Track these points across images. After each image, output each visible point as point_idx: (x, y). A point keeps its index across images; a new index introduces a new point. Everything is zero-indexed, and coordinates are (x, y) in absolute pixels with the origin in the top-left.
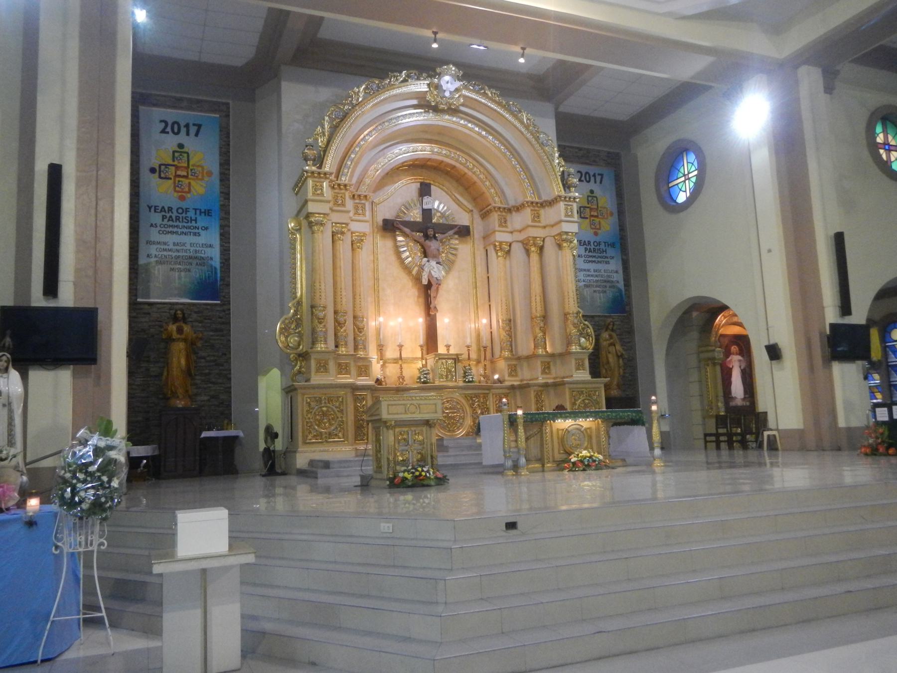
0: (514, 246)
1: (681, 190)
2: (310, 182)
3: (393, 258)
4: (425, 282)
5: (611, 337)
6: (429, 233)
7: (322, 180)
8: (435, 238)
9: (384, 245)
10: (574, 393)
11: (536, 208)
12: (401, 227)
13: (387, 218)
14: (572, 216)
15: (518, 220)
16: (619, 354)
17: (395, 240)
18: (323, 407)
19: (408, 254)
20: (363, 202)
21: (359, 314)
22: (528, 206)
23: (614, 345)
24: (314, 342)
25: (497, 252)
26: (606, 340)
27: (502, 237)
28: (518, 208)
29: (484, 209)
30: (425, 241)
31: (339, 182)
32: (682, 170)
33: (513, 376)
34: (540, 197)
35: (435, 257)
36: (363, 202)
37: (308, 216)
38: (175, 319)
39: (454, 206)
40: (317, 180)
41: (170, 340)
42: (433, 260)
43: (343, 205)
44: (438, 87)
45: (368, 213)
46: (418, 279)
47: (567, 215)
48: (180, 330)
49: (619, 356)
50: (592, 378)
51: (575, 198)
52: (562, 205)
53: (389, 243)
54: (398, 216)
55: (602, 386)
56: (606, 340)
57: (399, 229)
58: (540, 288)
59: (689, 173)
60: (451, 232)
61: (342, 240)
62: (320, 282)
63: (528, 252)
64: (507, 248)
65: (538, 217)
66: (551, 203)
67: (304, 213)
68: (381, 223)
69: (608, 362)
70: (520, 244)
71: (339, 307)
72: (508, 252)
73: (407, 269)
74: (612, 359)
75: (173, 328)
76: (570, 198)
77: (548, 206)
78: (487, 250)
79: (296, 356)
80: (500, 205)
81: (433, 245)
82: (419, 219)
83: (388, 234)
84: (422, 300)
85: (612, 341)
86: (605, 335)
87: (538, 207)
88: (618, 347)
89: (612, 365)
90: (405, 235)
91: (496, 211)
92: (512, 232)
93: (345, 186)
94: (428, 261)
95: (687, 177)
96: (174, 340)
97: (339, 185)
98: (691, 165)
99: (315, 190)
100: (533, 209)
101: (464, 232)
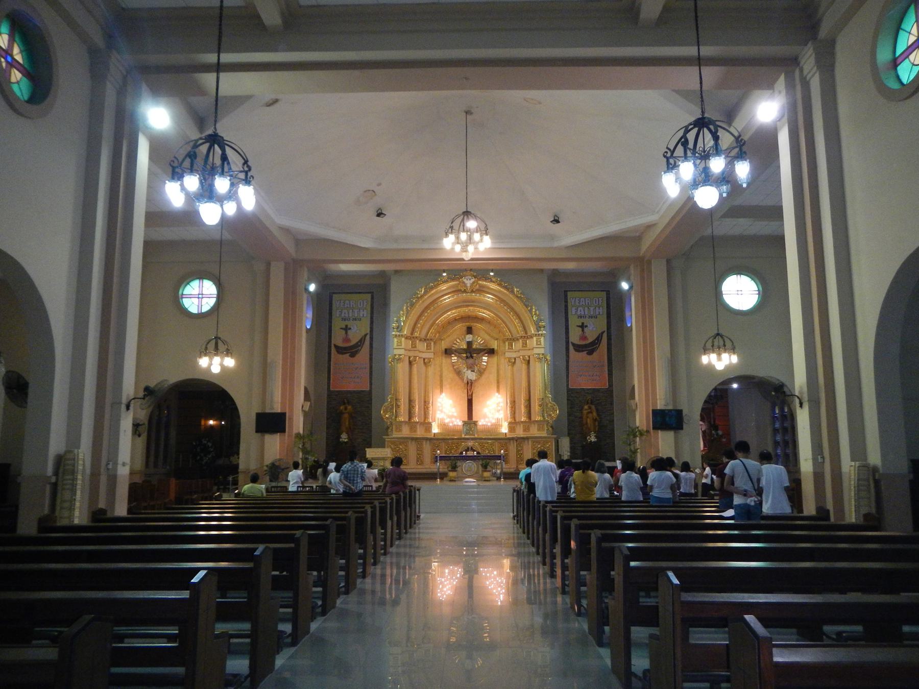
3: (452, 369)
4: (465, 381)
5: (590, 408)
8: (472, 357)
9: (445, 361)
10: (534, 444)
12: (455, 353)
15: (517, 345)
21: (427, 400)
23: (592, 413)
26: (586, 410)
27: (508, 355)
28: (518, 340)
31: (413, 336)
34: (526, 333)
35: (471, 368)
38: (344, 403)
41: (342, 413)
43: (415, 347)
44: (464, 283)
47: (537, 344)
48: (346, 409)
49: (595, 420)
51: (542, 334)
52: (535, 338)
53: (448, 360)
55: (553, 439)
56: (586, 410)
58: (527, 384)
64: (513, 360)
66: (532, 337)
68: (443, 349)
69: (587, 423)
71: (412, 398)
72: (515, 361)
75: (342, 408)
76: (539, 334)
81: (471, 361)
82: (465, 347)
84: (466, 391)
85: (589, 410)
86: (586, 407)
88: (595, 414)
89: (589, 426)
90: (456, 356)
93: (416, 337)
96: (344, 413)
97: (413, 337)
101: (491, 352)
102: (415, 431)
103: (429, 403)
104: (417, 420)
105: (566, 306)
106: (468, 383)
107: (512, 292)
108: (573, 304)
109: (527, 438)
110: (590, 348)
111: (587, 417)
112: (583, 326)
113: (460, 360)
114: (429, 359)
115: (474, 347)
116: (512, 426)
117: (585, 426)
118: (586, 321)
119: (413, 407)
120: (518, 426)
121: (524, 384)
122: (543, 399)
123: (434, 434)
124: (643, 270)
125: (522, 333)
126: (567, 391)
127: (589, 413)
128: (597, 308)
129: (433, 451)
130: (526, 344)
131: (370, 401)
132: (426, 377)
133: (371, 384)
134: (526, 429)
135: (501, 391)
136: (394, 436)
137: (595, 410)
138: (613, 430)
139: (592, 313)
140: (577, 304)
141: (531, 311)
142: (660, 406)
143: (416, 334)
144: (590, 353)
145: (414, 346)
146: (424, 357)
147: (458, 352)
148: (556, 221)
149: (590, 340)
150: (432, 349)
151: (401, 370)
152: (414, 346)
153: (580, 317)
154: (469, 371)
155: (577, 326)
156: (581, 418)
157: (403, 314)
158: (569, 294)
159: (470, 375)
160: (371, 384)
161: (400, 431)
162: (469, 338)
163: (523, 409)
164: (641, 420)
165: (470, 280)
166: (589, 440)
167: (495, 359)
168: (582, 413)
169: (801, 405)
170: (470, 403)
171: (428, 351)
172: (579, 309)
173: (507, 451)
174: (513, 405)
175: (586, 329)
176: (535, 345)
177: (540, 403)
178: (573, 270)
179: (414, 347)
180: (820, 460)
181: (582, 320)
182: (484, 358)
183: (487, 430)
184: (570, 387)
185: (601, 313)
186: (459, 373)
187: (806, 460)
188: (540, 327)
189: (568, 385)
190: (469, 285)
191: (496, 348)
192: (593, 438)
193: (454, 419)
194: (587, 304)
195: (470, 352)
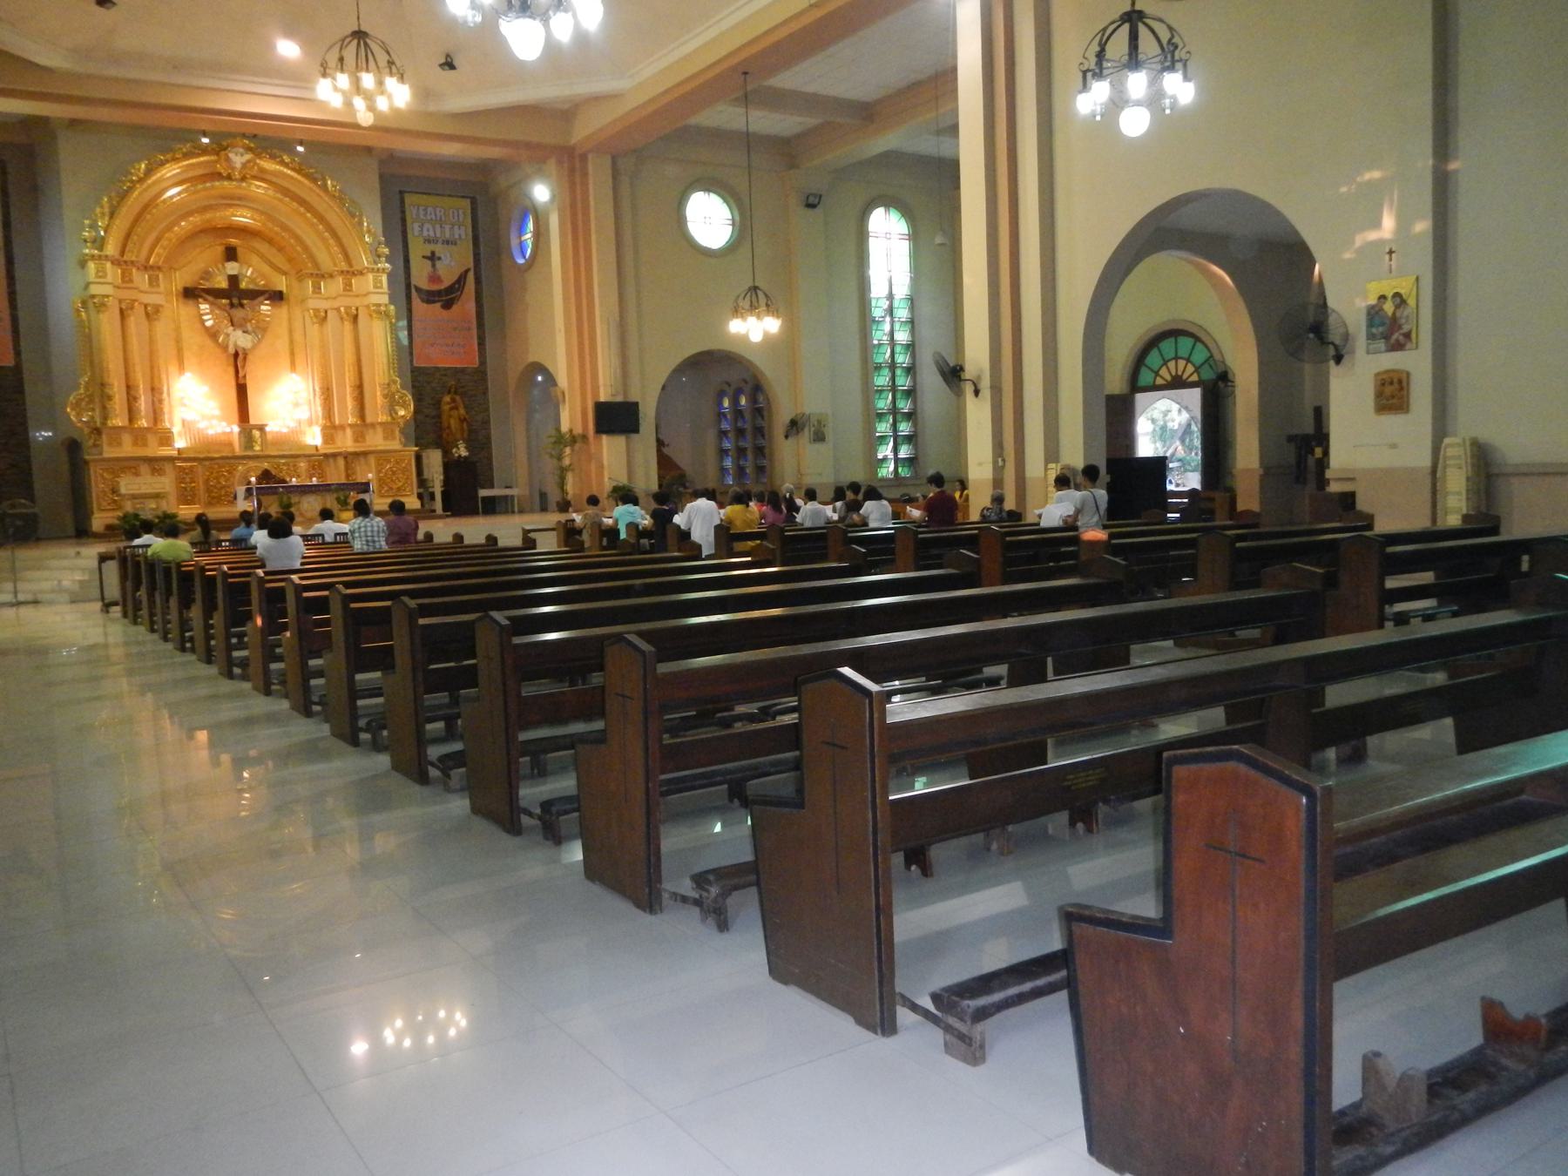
0: (329, 312)
3: (198, 325)
4: (231, 350)
5: (453, 400)
7: (104, 262)
8: (242, 306)
9: (185, 310)
10: (381, 462)
12: (204, 295)
13: (188, 285)
14: (381, 287)
16: (462, 417)
17: (199, 308)
22: (340, 275)
26: (448, 403)
27: (313, 303)
28: (331, 276)
31: (125, 258)
33: (329, 444)
34: (351, 265)
39: (266, 269)
43: (131, 281)
46: (225, 348)
47: (375, 287)
49: (462, 420)
51: (383, 269)
56: (448, 403)
57: (201, 297)
60: (261, 299)
64: (323, 314)
68: (180, 288)
69: (449, 424)
70: (335, 312)
71: (130, 384)
72: (325, 318)
74: (453, 423)
76: (378, 269)
80: (312, 272)
81: (238, 314)
82: (224, 284)
83: (191, 302)
84: (231, 370)
85: (453, 405)
86: (447, 399)
88: (462, 411)
89: (454, 430)
97: (125, 262)
101: (277, 297)
102: (145, 445)
103: (161, 393)
104: (144, 423)
105: (404, 220)
106: (236, 355)
107: (324, 187)
108: (414, 216)
109: (365, 454)
110: (446, 297)
111: (450, 416)
112: (432, 258)
113: (217, 312)
114: (157, 309)
115: (243, 285)
116: (331, 430)
117: (447, 431)
118: (439, 249)
119: (136, 399)
120: (340, 433)
121: (349, 357)
122: (388, 384)
123: (179, 450)
124: (572, 171)
125: (344, 266)
126: (412, 372)
127: (451, 409)
128: (456, 227)
129: (181, 482)
130: (351, 285)
131: (19, 389)
132: (152, 341)
133: (18, 353)
134: (359, 437)
135: (299, 367)
136: (106, 455)
137: (462, 406)
138: (488, 438)
139: (447, 235)
140: (422, 217)
141: (361, 224)
142: (602, 399)
143: (128, 257)
144: (448, 305)
145: (127, 279)
146: (146, 301)
147: (216, 294)
148: (449, 65)
149: (446, 283)
150: (162, 285)
151: (107, 326)
152: (127, 279)
153: (428, 241)
154: (239, 333)
155: (424, 257)
156: (439, 416)
157: (103, 214)
158: (408, 199)
159: (240, 339)
160: (18, 353)
161: (120, 444)
162: (232, 268)
163: (350, 404)
164: (572, 417)
165: (242, 155)
166: (456, 455)
167: (283, 311)
168: (439, 408)
169: (977, 392)
170: (242, 391)
171: (153, 290)
172: (427, 226)
173: (322, 477)
174: (327, 394)
175: (438, 264)
176: (371, 289)
177: (386, 392)
178: (454, 156)
179: (127, 282)
180: (1000, 463)
181: (432, 247)
182: (263, 307)
183: (280, 440)
184: (415, 365)
185: (463, 237)
186: (213, 334)
187: (980, 464)
188: (379, 256)
189: (412, 365)
190: (238, 166)
191: (284, 290)
192: (463, 451)
193: (215, 422)
194: (438, 218)
195: (235, 296)
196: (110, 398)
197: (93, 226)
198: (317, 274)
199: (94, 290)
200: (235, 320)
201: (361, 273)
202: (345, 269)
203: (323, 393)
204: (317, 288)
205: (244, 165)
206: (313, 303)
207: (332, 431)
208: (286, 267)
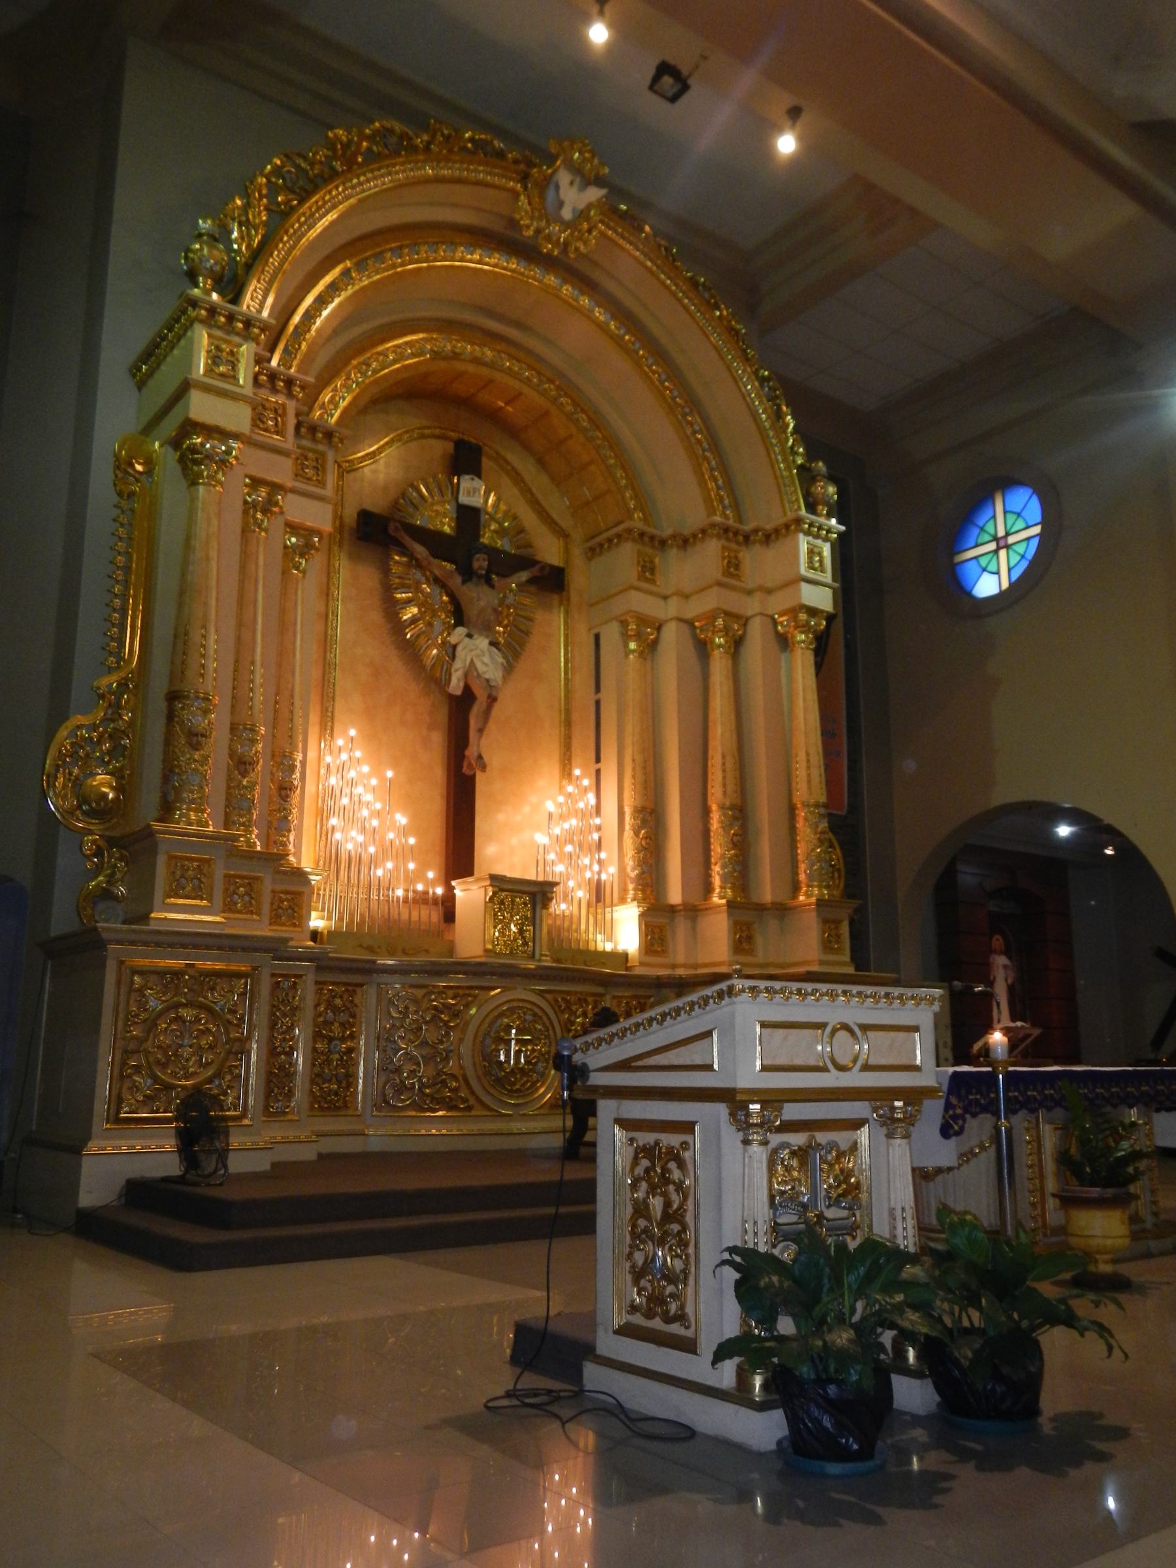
1: (984, 570)
2: (202, 338)
3: (376, 616)
4: (456, 686)
6: (476, 565)
7: (236, 339)
11: (733, 546)
13: (369, 506)
18: (185, 1006)
19: (413, 611)
20: (320, 447)
22: (719, 537)
24: (167, 810)
25: (626, 637)
28: (685, 542)
29: (600, 533)
30: (464, 582)
32: (990, 528)
36: (320, 447)
37: (190, 427)
39: (529, 518)
40: (219, 333)
42: (480, 634)
45: (331, 479)
50: (857, 970)
54: (395, 505)
59: (1007, 534)
60: (524, 576)
61: (266, 531)
62: (204, 627)
63: (703, 649)
65: (737, 567)
67: (170, 426)
72: (654, 644)
73: (410, 652)
76: (820, 528)
77: (760, 542)
78: (597, 637)
79: (101, 843)
84: (439, 738)
87: (738, 543)
91: (634, 540)
92: (665, 598)
94: (469, 636)
95: (1002, 543)
98: (1015, 517)
99: (214, 363)
100: (726, 544)
190: (567, 214)
196: (196, 739)
197: (220, 237)
198: (652, 538)
199: (200, 407)
200: (471, 612)
201: (769, 538)
202: (731, 522)
203: (644, 823)
204: (648, 570)
205: (582, 215)
206: (640, 602)
207: (662, 920)
208: (566, 522)
